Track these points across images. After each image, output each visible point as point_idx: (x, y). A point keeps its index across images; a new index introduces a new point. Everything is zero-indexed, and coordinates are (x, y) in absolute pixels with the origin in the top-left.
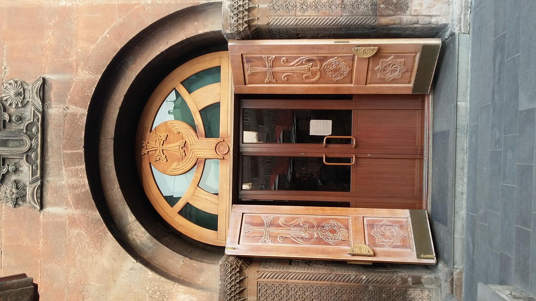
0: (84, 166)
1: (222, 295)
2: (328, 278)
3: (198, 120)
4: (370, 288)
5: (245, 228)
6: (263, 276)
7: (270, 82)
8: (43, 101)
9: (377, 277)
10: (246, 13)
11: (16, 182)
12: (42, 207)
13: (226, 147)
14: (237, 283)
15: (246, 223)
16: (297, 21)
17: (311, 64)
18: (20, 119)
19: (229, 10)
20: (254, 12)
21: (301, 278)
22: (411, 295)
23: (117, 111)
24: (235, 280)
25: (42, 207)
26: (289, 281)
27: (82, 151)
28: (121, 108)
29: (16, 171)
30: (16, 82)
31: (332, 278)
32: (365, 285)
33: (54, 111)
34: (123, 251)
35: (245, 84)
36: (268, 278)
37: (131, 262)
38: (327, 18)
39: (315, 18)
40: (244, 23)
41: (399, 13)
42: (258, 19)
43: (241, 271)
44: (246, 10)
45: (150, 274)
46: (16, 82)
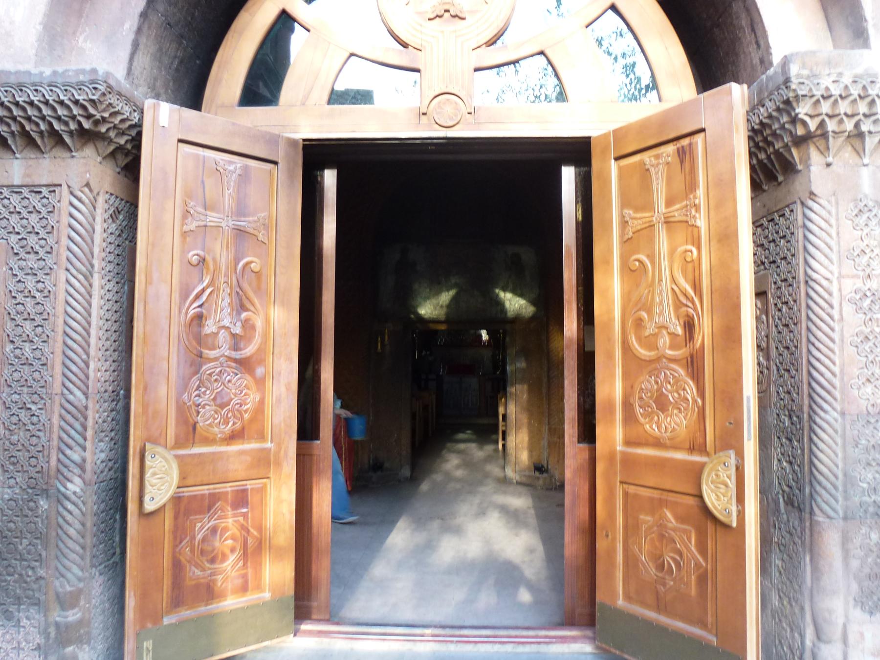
1: (13, 80)
2: (71, 386)
4: (43, 503)
5: (230, 163)
6: (76, 202)
7: (624, 223)
9: (78, 526)
10: (849, 125)
13: (451, 119)
14: (50, 124)
15: (246, 168)
16: (825, 283)
17: (680, 331)
19: (859, 70)
20: (848, 153)
21: (69, 309)
22: (28, 618)
24: (59, 119)
26: (63, 275)
31: (71, 397)
32: (52, 491)
35: (616, 159)
36: (71, 215)
38: (836, 369)
39: (836, 336)
40: (817, 120)
41: (855, 587)
42: (828, 165)
43: (86, 136)
44: (857, 125)
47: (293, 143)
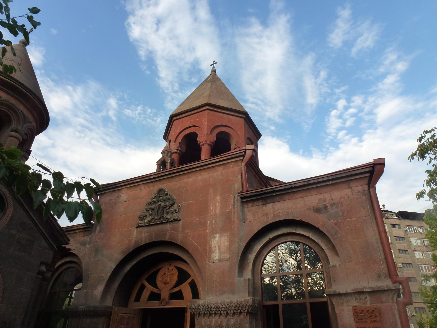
0: (148, 242)
3: (177, 289)
8: (172, 221)
11: (146, 216)
12: (137, 227)
18: (168, 213)
23: (171, 252)
25: (137, 227)
27: (153, 241)
28: (172, 254)
29: (151, 215)
30: (180, 209)
33: (168, 226)
34: (118, 263)
37: (114, 266)
45: (109, 275)
46: (180, 209)
47: (139, 310)
